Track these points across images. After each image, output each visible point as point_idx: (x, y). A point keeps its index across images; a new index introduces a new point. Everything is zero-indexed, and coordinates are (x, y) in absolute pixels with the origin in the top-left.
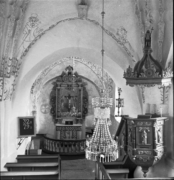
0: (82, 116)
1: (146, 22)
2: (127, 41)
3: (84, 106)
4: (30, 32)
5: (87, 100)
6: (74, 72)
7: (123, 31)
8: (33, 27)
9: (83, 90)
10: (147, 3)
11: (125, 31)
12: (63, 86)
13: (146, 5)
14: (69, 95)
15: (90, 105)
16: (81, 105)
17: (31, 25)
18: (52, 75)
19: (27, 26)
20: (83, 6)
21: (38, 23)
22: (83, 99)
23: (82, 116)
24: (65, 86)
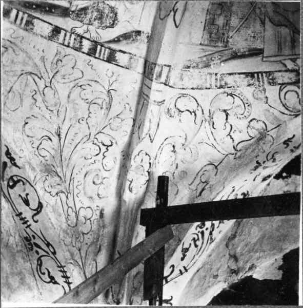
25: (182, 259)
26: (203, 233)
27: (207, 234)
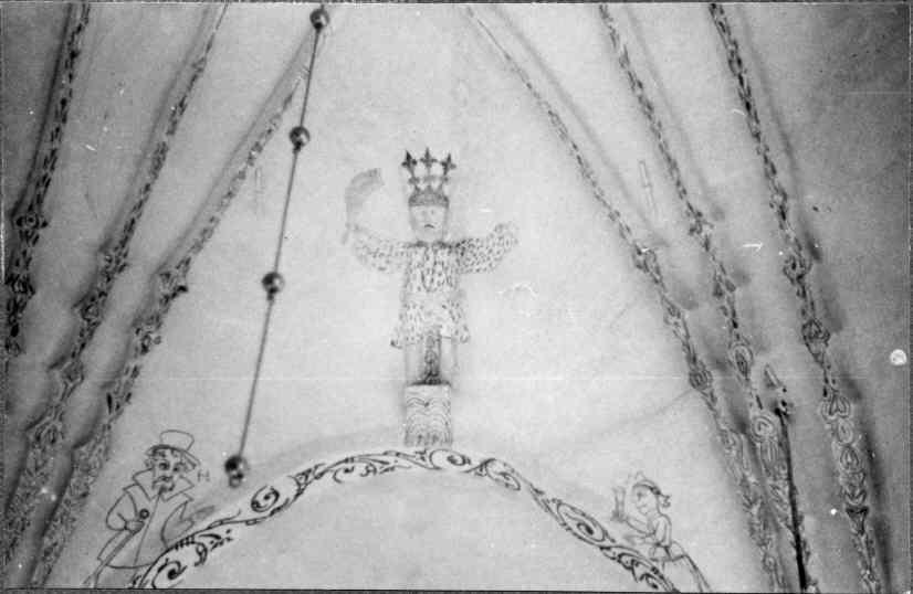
1: (754, 412)
2: (676, 551)
4: (147, 521)
7: (649, 497)
8: (166, 495)
10: (734, 314)
11: (658, 493)
13: (735, 325)
17: (153, 487)
19: (136, 491)
20: (427, 391)
21: (192, 475)
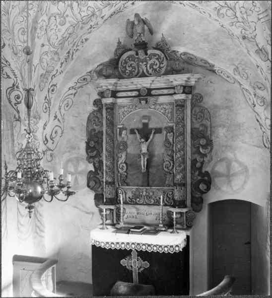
0: (192, 202)
3: (198, 165)
5: (209, 143)
6: (158, 37)
9: (193, 106)
12: (124, 94)
14: (145, 125)
15: (224, 164)
16: (184, 161)
18: (88, 62)
22: (193, 137)
23: (189, 202)
24: (129, 94)
25: (61, 67)
26: (69, 56)
27: (70, 57)
